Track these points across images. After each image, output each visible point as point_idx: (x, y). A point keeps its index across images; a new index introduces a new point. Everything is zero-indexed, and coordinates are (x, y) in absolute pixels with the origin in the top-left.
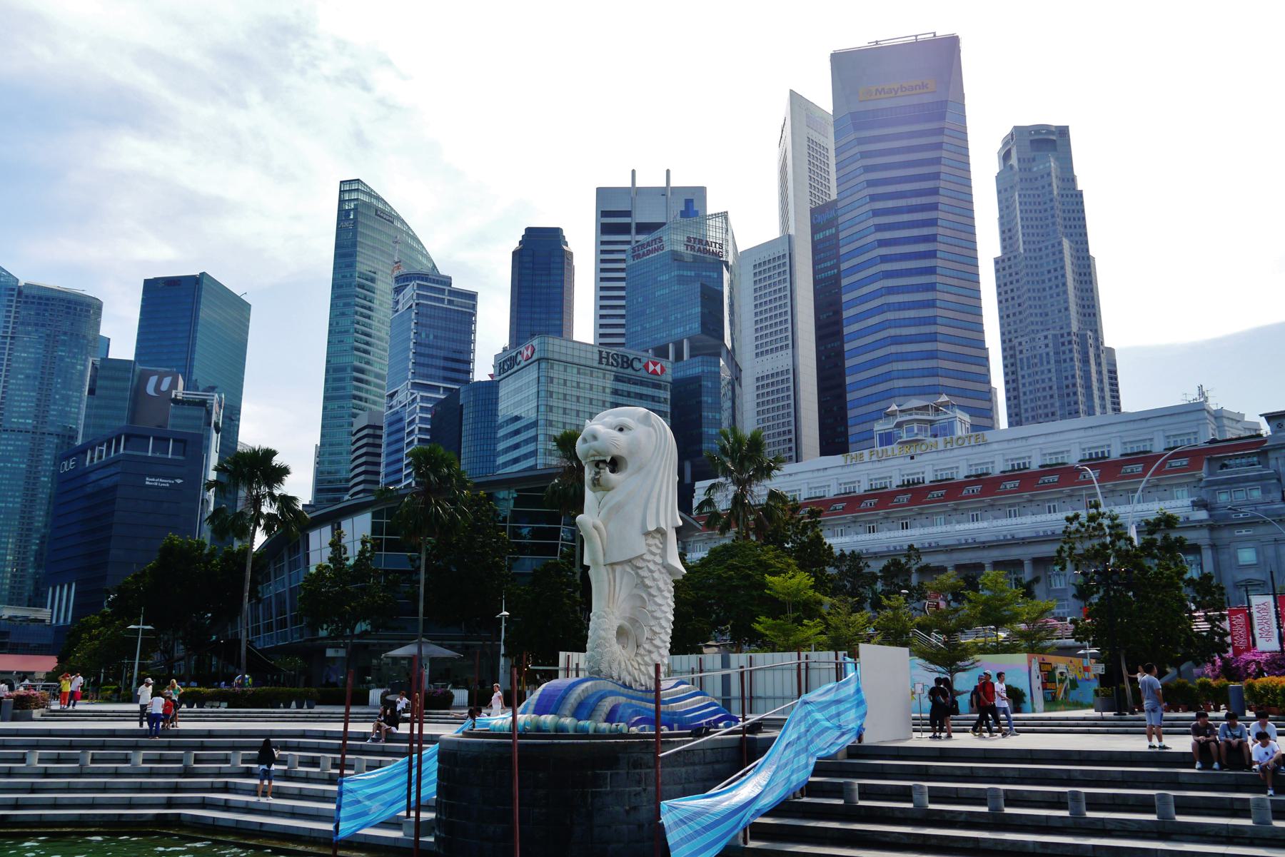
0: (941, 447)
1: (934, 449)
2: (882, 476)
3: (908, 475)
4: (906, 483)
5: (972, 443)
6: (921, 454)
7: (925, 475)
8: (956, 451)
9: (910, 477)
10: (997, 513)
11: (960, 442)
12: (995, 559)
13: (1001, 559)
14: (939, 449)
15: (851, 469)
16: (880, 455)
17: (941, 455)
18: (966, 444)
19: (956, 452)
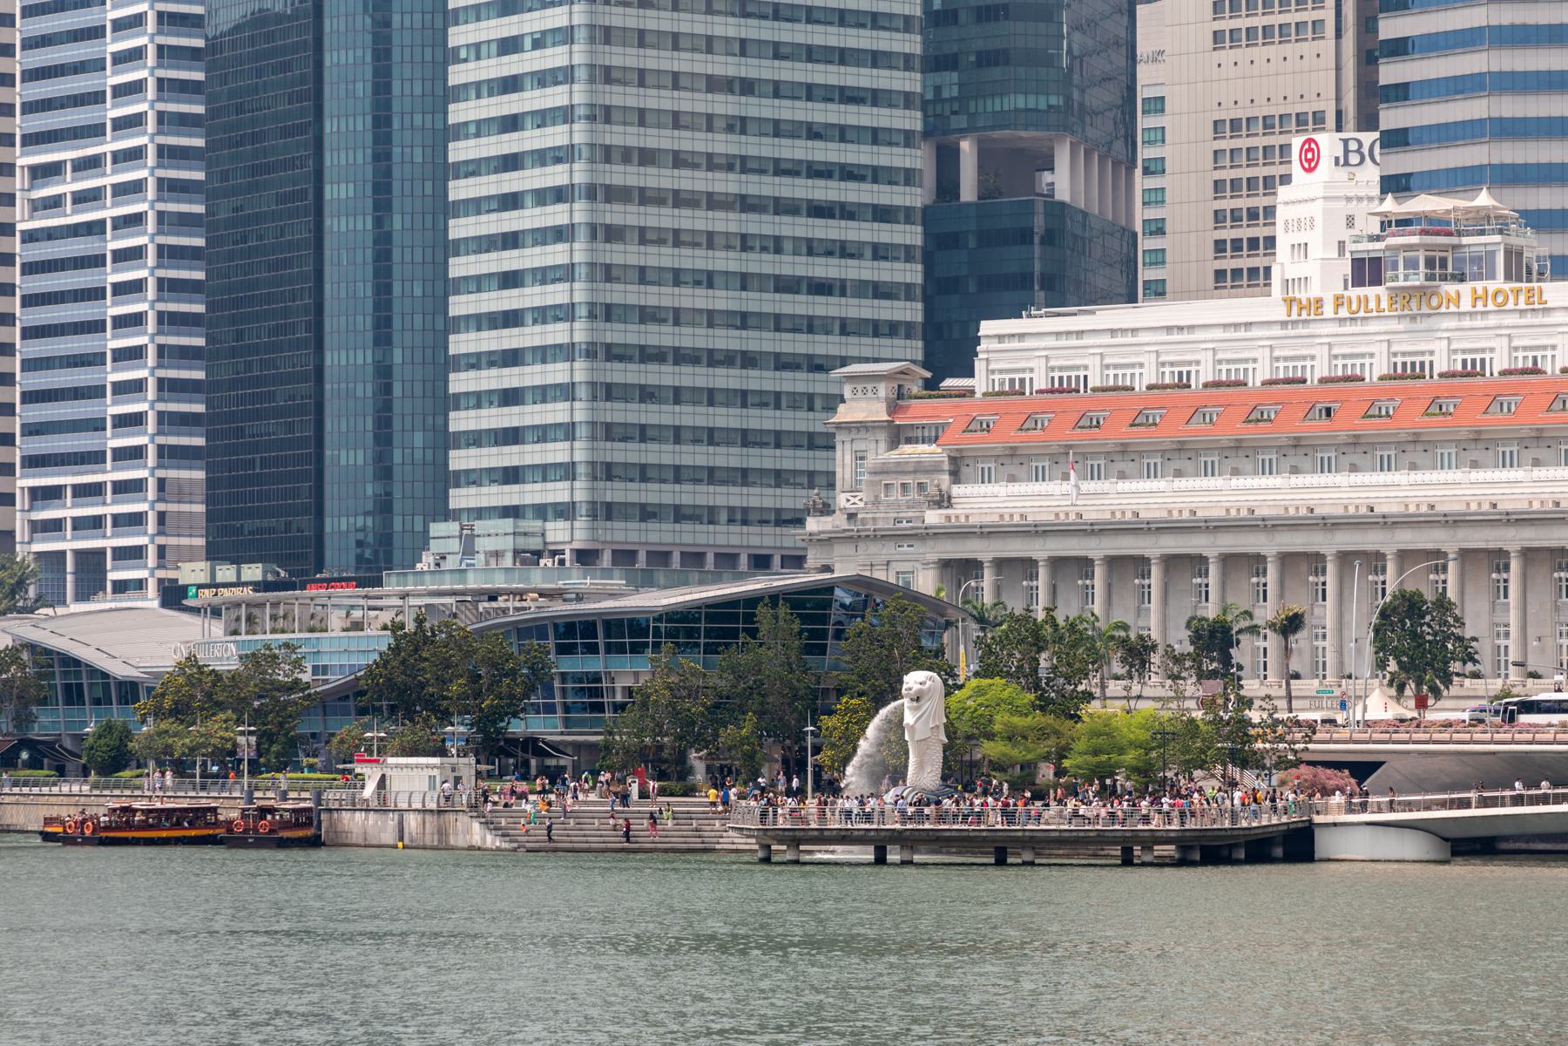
0: (1466, 305)
1: (1453, 309)
2: (1356, 351)
3: (1404, 354)
4: (1399, 370)
5: (1522, 305)
6: (1429, 315)
7: (1435, 358)
8: (1491, 316)
9: (1409, 360)
10: (1542, 453)
11: (1500, 299)
12: (1527, 544)
13: (1536, 544)
14: (1462, 309)
15: (1301, 331)
16: (1354, 307)
17: (1467, 323)
18: (1510, 306)
19: (1492, 321)
